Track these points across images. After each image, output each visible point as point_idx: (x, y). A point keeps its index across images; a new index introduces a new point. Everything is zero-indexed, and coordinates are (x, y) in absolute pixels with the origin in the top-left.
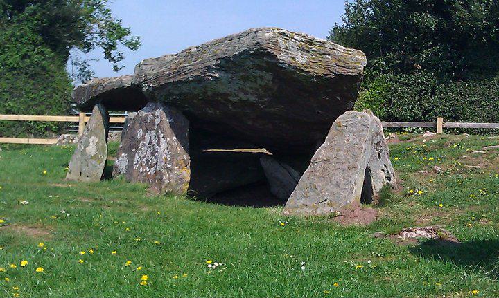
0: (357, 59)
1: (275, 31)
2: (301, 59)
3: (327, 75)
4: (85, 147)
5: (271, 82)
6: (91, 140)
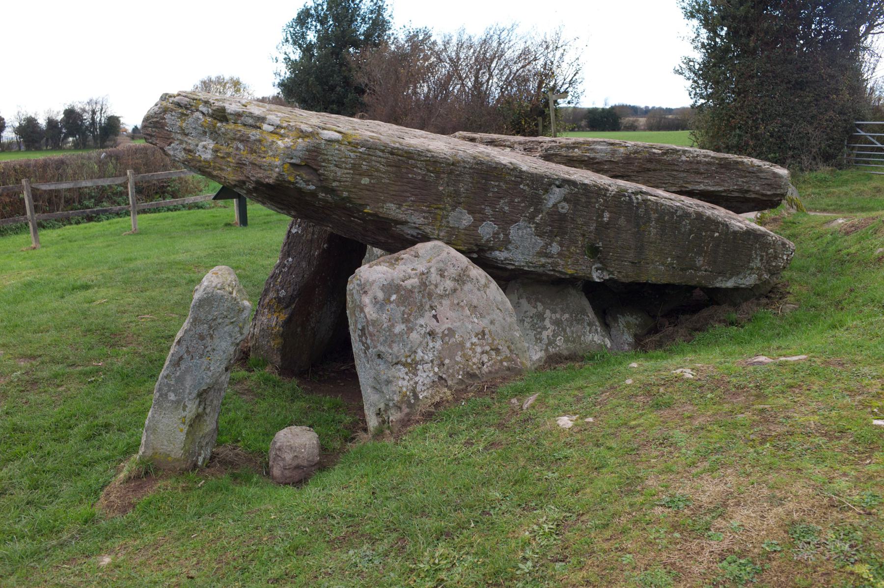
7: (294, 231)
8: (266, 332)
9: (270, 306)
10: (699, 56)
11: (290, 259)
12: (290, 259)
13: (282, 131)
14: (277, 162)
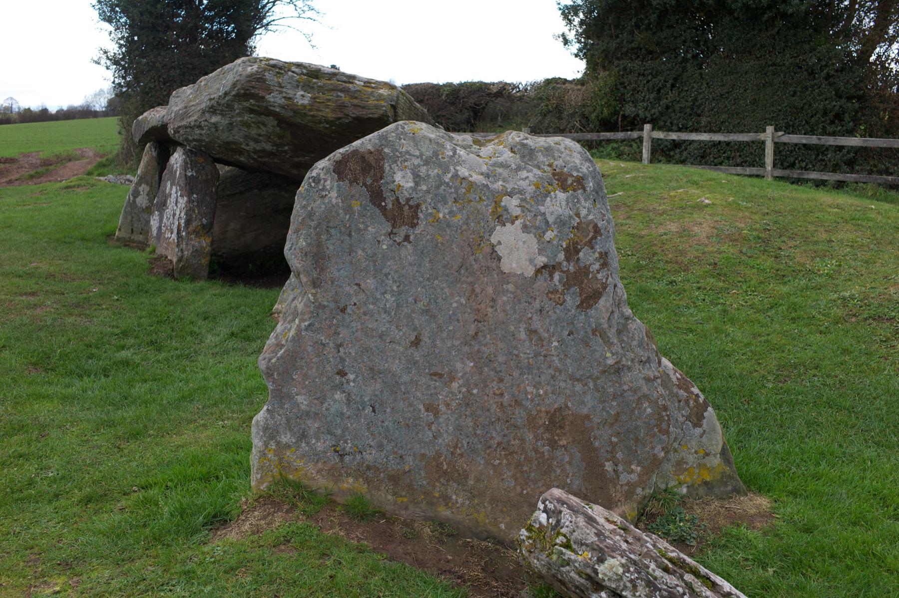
0: (381, 95)
1: (264, 63)
2: (302, 98)
3: (340, 118)
4: (135, 197)
5: (278, 129)
6: (141, 189)
7: (189, 174)
8: (197, 253)
9: (197, 233)
10: (113, 49)
11: (195, 196)
12: (195, 196)
13: (373, 85)
14: (383, 103)
